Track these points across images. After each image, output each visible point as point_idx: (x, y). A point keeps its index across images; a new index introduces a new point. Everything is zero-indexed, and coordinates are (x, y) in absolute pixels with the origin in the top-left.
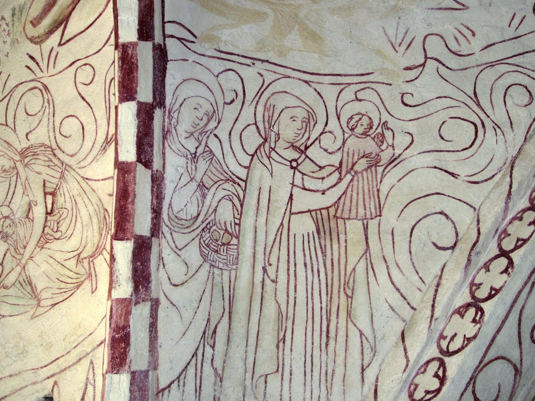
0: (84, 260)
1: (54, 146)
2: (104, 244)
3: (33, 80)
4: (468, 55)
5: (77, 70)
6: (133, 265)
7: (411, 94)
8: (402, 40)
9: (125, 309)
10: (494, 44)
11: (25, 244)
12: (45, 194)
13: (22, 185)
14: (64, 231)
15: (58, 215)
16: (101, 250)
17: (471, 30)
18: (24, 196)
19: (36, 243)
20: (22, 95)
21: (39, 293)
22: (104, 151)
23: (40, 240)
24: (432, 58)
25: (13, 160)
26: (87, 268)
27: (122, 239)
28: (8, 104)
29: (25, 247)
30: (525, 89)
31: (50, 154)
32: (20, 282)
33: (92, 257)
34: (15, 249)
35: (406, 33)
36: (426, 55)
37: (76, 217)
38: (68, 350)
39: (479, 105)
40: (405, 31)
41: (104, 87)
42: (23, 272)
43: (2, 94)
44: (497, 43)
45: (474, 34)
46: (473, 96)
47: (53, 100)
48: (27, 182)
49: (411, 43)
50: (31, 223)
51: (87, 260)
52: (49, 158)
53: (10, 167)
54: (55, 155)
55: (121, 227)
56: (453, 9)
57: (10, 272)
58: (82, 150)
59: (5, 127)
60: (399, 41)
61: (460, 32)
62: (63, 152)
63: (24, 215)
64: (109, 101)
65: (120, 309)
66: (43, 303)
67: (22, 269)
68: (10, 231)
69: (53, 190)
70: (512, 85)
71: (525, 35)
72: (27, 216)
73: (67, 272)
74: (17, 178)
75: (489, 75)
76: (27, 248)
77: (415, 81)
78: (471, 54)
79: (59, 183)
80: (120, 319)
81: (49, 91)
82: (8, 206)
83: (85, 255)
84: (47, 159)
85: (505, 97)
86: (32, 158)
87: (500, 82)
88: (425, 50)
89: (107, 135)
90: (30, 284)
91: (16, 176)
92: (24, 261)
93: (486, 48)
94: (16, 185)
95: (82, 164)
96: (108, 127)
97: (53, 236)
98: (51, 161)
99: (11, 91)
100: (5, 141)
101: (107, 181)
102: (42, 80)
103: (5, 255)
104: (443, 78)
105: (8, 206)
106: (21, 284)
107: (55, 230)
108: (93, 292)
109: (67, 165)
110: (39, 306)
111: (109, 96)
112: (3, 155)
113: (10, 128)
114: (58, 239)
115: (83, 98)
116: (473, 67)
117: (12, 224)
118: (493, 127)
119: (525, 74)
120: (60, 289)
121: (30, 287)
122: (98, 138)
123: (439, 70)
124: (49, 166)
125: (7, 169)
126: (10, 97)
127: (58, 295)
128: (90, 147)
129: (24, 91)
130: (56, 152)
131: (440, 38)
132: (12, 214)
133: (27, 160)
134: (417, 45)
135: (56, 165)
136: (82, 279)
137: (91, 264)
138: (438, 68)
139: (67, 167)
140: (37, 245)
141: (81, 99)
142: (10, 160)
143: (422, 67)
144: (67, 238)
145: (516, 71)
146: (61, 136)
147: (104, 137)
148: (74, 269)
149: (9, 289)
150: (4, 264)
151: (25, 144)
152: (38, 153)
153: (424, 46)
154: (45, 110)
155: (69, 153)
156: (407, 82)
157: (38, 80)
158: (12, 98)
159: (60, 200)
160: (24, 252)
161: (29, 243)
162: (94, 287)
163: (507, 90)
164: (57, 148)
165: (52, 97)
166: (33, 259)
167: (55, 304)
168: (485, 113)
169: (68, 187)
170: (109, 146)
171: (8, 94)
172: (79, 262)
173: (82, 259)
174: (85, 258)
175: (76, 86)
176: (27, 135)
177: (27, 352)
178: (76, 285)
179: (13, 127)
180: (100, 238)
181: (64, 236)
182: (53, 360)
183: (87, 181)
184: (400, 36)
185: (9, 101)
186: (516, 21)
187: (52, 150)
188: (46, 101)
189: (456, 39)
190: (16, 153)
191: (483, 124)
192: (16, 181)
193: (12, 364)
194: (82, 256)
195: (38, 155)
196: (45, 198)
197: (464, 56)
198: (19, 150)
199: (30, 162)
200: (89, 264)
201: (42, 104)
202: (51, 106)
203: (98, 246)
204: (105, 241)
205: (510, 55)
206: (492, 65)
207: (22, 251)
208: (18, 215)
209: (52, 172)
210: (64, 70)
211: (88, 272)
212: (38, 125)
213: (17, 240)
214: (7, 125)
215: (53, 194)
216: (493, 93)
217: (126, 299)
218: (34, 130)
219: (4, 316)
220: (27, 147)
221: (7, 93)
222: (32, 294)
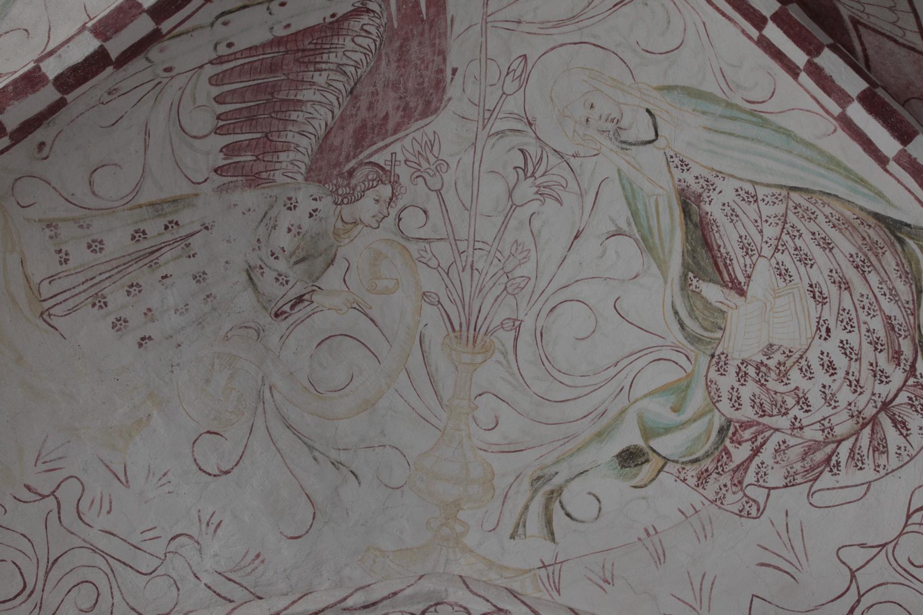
4: (86, 524)
7: (5, 510)
8: (50, 461)
10: (115, 535)
17: (111, 507)
24: (56, 498)
30: (96, 595)
35: (60, 458)
36: (54, 491)
39: (47, 573)
40: (61, 456)
44: (118, 537)
45: (109, 512)
46: (51, 562)
49: (55, 470)
56: (116, 476)
60: (47, 459)
61: (101, 499)
70: (90, 582)
71: (145, 552)
75: (83, 556)
77: (22, 503)
78: (89, 525)
85: (74, 586)
87: (86, 570)
88: (59, 486)
93: (106, 532)
104: (46, 523)
116: (79, 537)
118: (36, 604)
119: (110, 583)
123: (51, 513)
131: (81, 489)
134: (58, 476)
138: (51, 511)
143: (40, 498)
145: (107, 574)
153: (62, 482)
156: (15, 498)
163: (83, 582)
168: (44, 585)
184: (53, 456)
186: (150, 535)
189: (93, 502)
191: (32, 592)
197: (83, 521)
205: (116, 557)
206: (95, 550)
216: (69, 575)
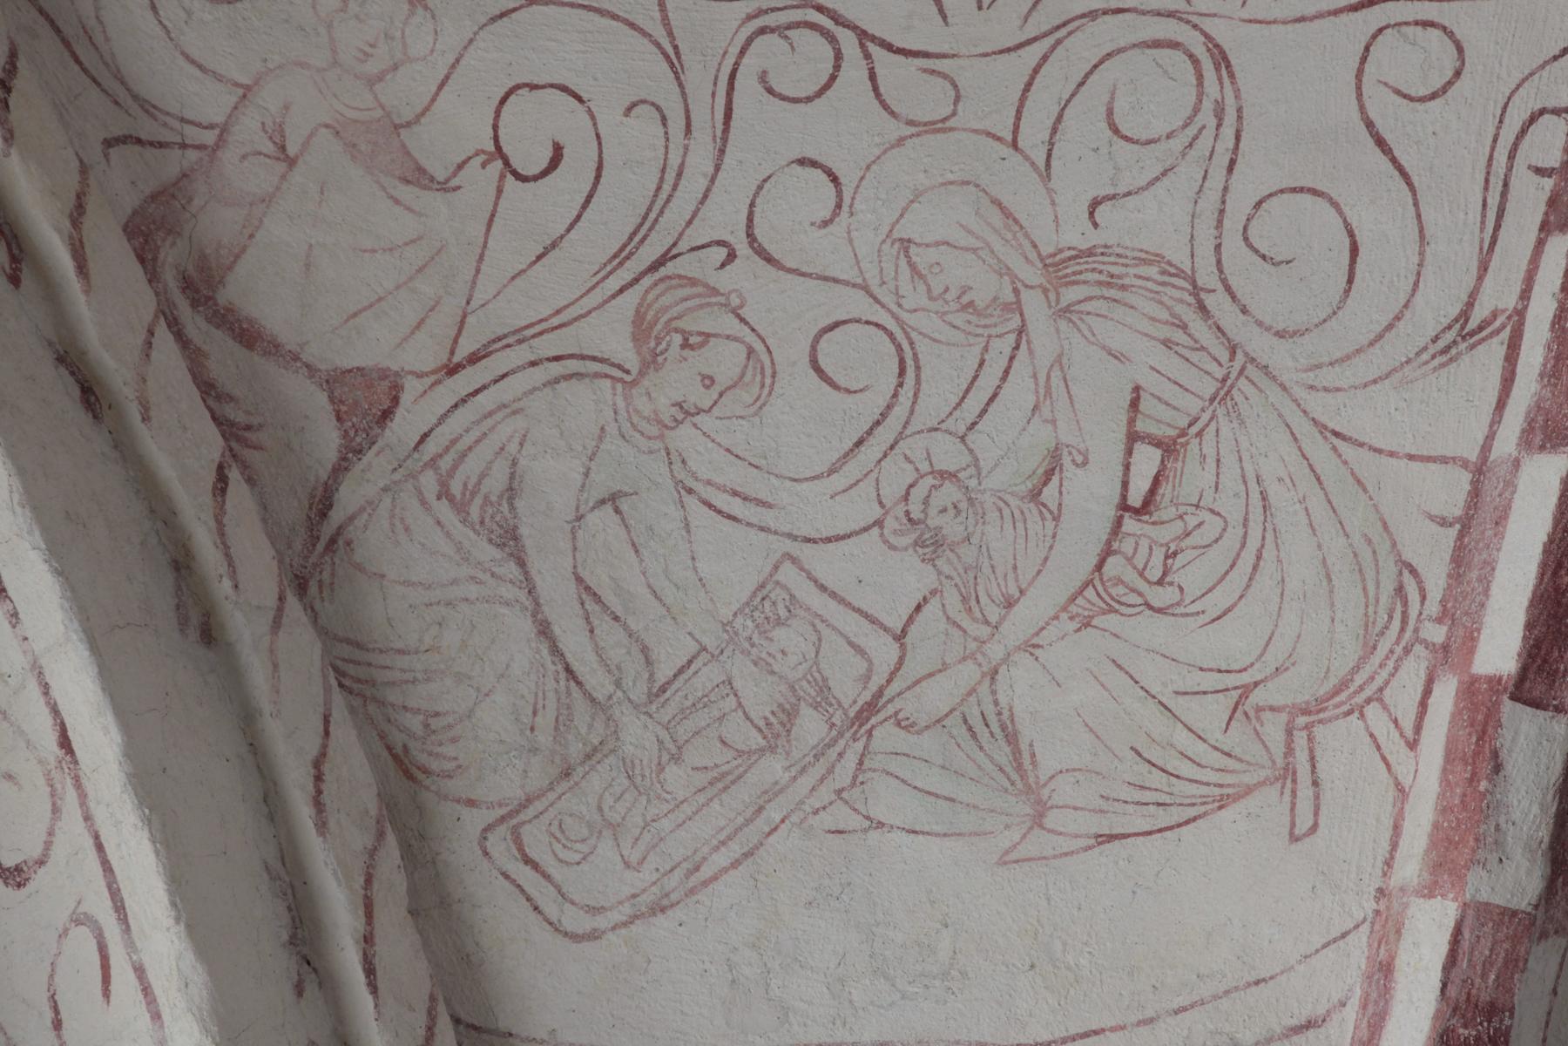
0: (1267, 715)
1: (1207, 276)
2: (1379, 681)
3: (1171, 14)
5: (1380, 30)
6: (1560, 803)
9: (1506, 946)
11: (1015, 593)
12: (1133, 438)
13: (1035, 376)
14: (1192, 591)
15: (1178, 528)
16: (1359, 699)
18: (1036, 419)
19: (1063, 600)
20: (1109, 55)
21: (1043, 779)
22: (1444, 358)
23: (1080, 592)
25: (1014, 278)
26: (1278, 750)
27: (1537, 704)
28: (1036, 71)
29: (1009, 604)
31: (1181, 301)
32: (965, 721)
33: (1306, 712)
34: (964, 600)
37: (1259, 557)
38: (1150, 1013)
41: (1491, 131)
42: (984, 688)
43: (1021, 27)
47: (1240, 110)
48: (1056, 374)
50: (1050, 524)
51: (1284, 717)
52: (1173, 315)
53: (995, 299)
54: (1202, 308)
55: (1545, 661)
57: (931, 675)
58: (1333, 323)
59: (1007, 151)
62: (1244, 311)
63: (1023, 489)
64: (1506, 185)
65: (1486, 944)
66: (1051, 820)
67: (984, 675)
68: (952, 528)
69: (1173, 433)
72: (1035, 495)
73: (1182, 738)
74: (1017, 347)
76: (1016, 609)
79: (1205, 417)
80: (1484, 976)
81: (1232, 75)
82: (963, 438)
83: (1278, 700)
84: (1165, 316)
86: (1096, 291)
89: (1470, 304)
90: (1012, 738)
91: (1012, 338)
92: (995, 651)
94: (1007, 372)
95: (1328, 377)
96: (1480, 278)
97: (1140, 594)
98: (1184, 327)
99: (1064, 25)
100: (997, 203)
101: (1432, 466)
102: (1208, 25)
103: (918, 608)
105: (963, 438)
106: (970, 729)
107: (1154, 574)
108: (1294, 838)
109: (1253, 360)
110: (1041, 826)
111: (1510, 168)
112: (974, 250)
113: (1027, 158)
114: (1159, 611)
115: (1380, 142)
117: (963, 505)
120: (1142, 787)
121: (1008, 750)
122: (1419, 297)
124: (1167, 343)
125: (980, 304)
126: (1053, 48)
127: (1130, 808)
128: (1379, 329)
129: (1122, 44)
130: (1209, 301)
132: (972, 470)
133: (1071, 295)
135: (1203, 348)
136: (1248, 779)
137: (1300, 739)
139: (1251, 370)
140: (1065, 609)
141: (1370, 142)
142: (1001, 275)
144: (1202, 619)
146: (1245, 249)
147: (1454, 311)
148: (1216, 736)
149: (919, 733)
150: (908, 640)
151: (1076, 234)
152: (1126, 281)
154: (1196, 138)
155: (1268, 321)
157: (1195, 19)
158: (1060, 50)
159: (1193, 477)
160: (1003, 619)
161: (1031, 592)
162: (1304, 823)
164: (1220, 287)
165: (1237, 97)
166: (1038, 652)
167: (1112, 838)
169: (1243, 439)
170: (1472, 347)
171: (1045, 35)
172: (1239, 714)
173: (1259, 709)
174: (1272, 709)
175: (1359, 88)
176: (1095, 204)
177: (964, 974)
178: (1217, 791)
179: (1041, 162)
180: (1363, 660)
181: (1192, 609)
182: (1073, 1031)
183: (1336, 441)
185: (1045, 58)
187: (1196, 290)
188: (1208, 105)
190: (1033, 256)
192: (1012, 358)
193: (892, 1004)
194: (1258, 697)
195: (1123, 288)
196: (1129, 452)
198: (1046, 250)
199: (1082, 307)
200: (1289, 732)
201: (1189, 111)
202: (1228, 132)
203: (1343, 685)
204: (1384, 674)
207: (994, 614)
208: (988, 483)
209: (1171, 364)
210: (1319, 16)
211: (1280, 762)
212: (1151, 183)
213: (978, 568)
214: (1015, 145)
215: (1169, 448)
217: (1514, 913)
218: (1129, 194)
219: (881, 825)
220: (1084, 247)
221: (1045, 28)
222: (1015, 776)
